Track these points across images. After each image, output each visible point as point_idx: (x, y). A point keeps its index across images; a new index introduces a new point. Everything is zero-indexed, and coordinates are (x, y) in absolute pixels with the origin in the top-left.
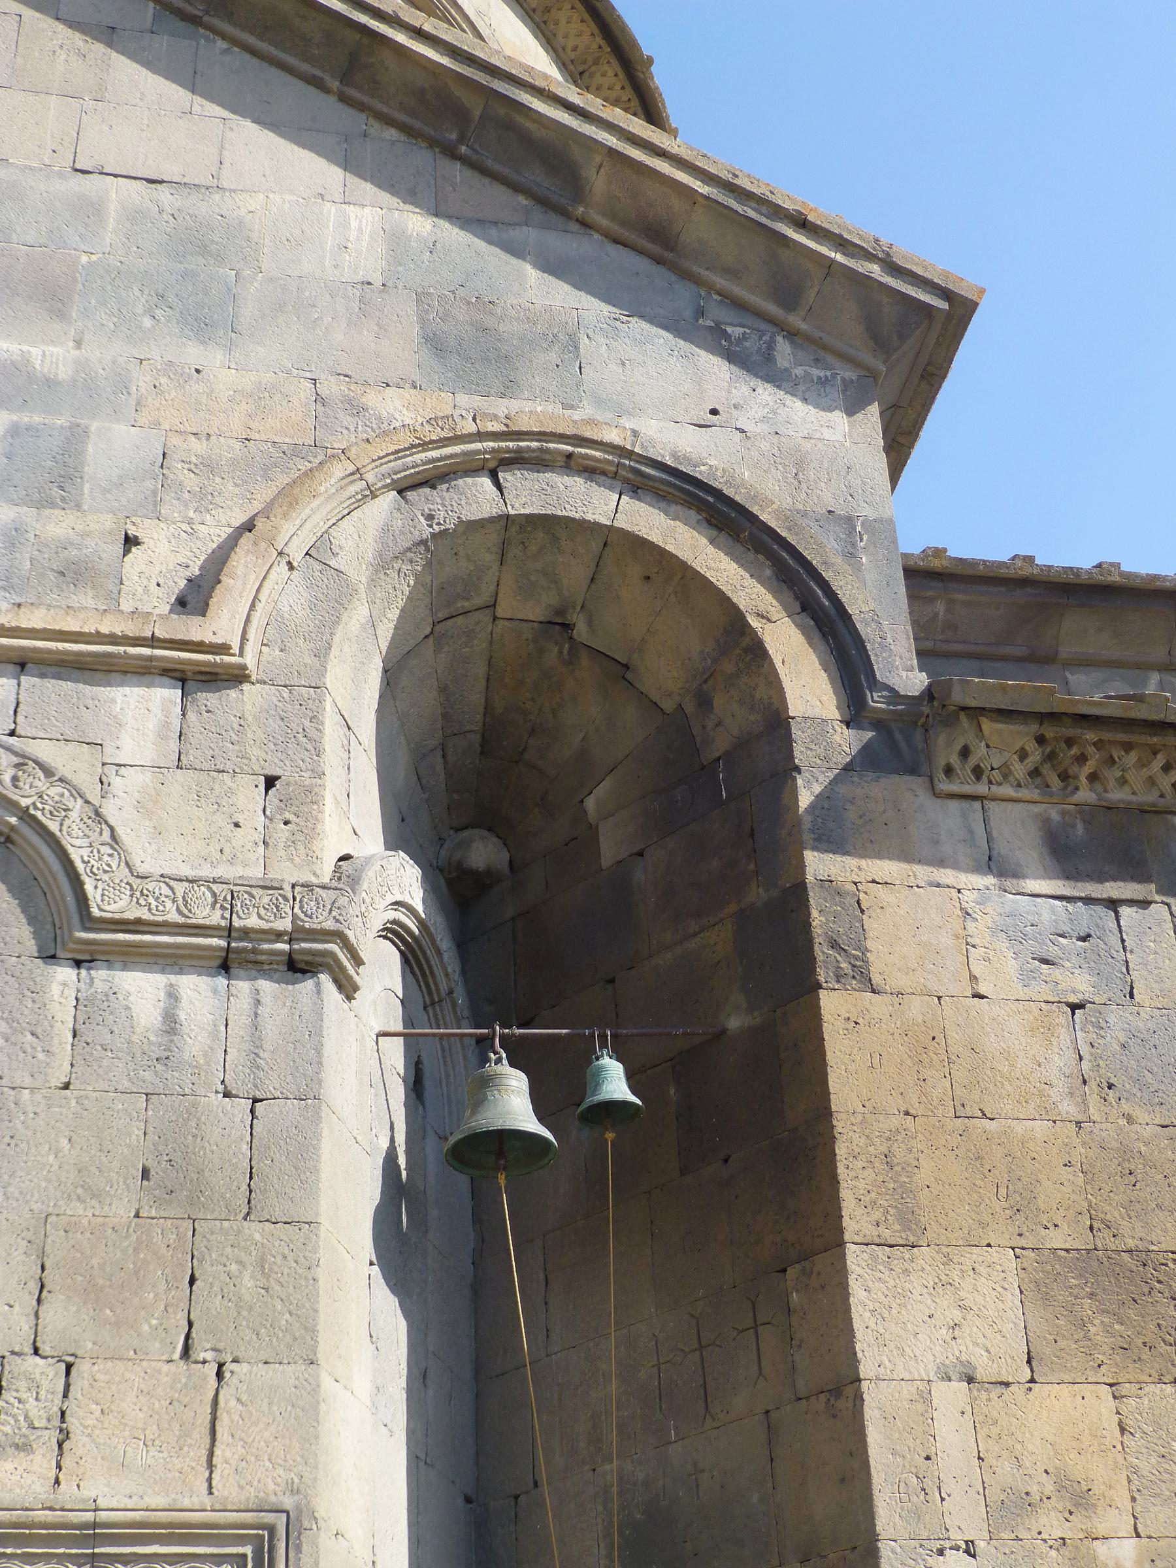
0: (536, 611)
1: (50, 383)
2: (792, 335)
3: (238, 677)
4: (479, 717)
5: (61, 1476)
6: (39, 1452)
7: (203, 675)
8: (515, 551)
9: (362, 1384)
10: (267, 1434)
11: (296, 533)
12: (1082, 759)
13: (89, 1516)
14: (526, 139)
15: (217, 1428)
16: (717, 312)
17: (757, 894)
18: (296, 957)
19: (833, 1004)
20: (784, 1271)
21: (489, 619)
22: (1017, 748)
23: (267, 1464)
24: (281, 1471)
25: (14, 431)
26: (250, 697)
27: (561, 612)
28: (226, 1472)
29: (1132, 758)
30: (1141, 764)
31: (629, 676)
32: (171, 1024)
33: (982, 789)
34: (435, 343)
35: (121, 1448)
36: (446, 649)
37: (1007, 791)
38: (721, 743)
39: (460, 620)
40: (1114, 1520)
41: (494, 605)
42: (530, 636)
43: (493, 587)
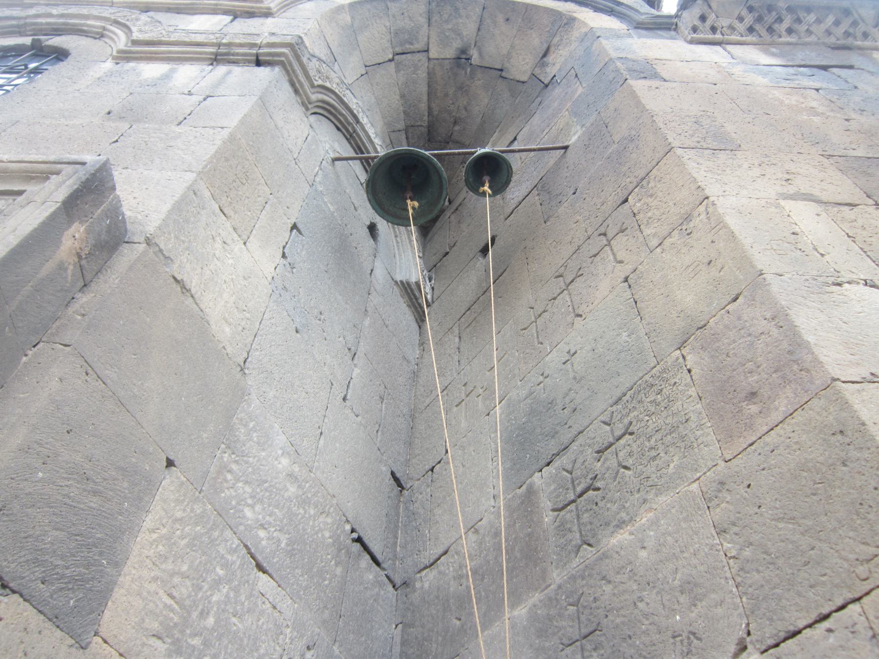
0: (450, 53)
4: (426, 118)
8: (435, 18)
12: (780, 20)
18: (260, 58)
20: (626, 200)
21: (425, 59)
22: (736, 16)
27: (463, 51)
29: (812, 18)
30: (819, 21)
31: (504, 74)
33: (718, 36)
36: (402, 72)
37: (735, 37)
39: (409, 56)
41: (427, 51)
42: (448, 67)
43: (426, 39)
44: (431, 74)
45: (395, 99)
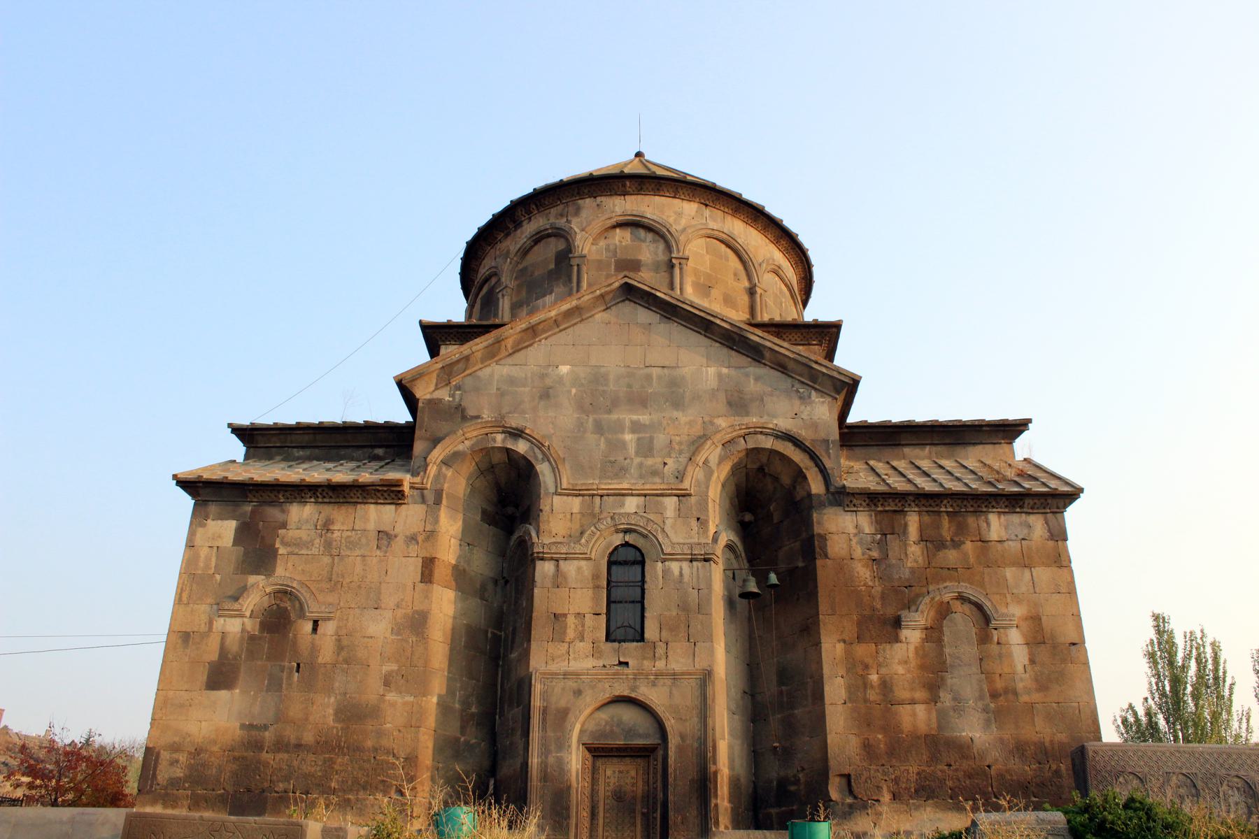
1: (645, 425)
2: (816, 389)
3: (690, 495)
7: (682, 496)
9: (723, 645)
11: (700, 459)
14: (750, 346)
16: (797, 385)
17: (804, 535)
19: (819, 563)
25: (639, 439)
26: (693, 500)
32: (681, 574)
34: (730, 404)
38: (798, 498)
40: (873, 671)
44: (747, 475)
45: (733, 487)
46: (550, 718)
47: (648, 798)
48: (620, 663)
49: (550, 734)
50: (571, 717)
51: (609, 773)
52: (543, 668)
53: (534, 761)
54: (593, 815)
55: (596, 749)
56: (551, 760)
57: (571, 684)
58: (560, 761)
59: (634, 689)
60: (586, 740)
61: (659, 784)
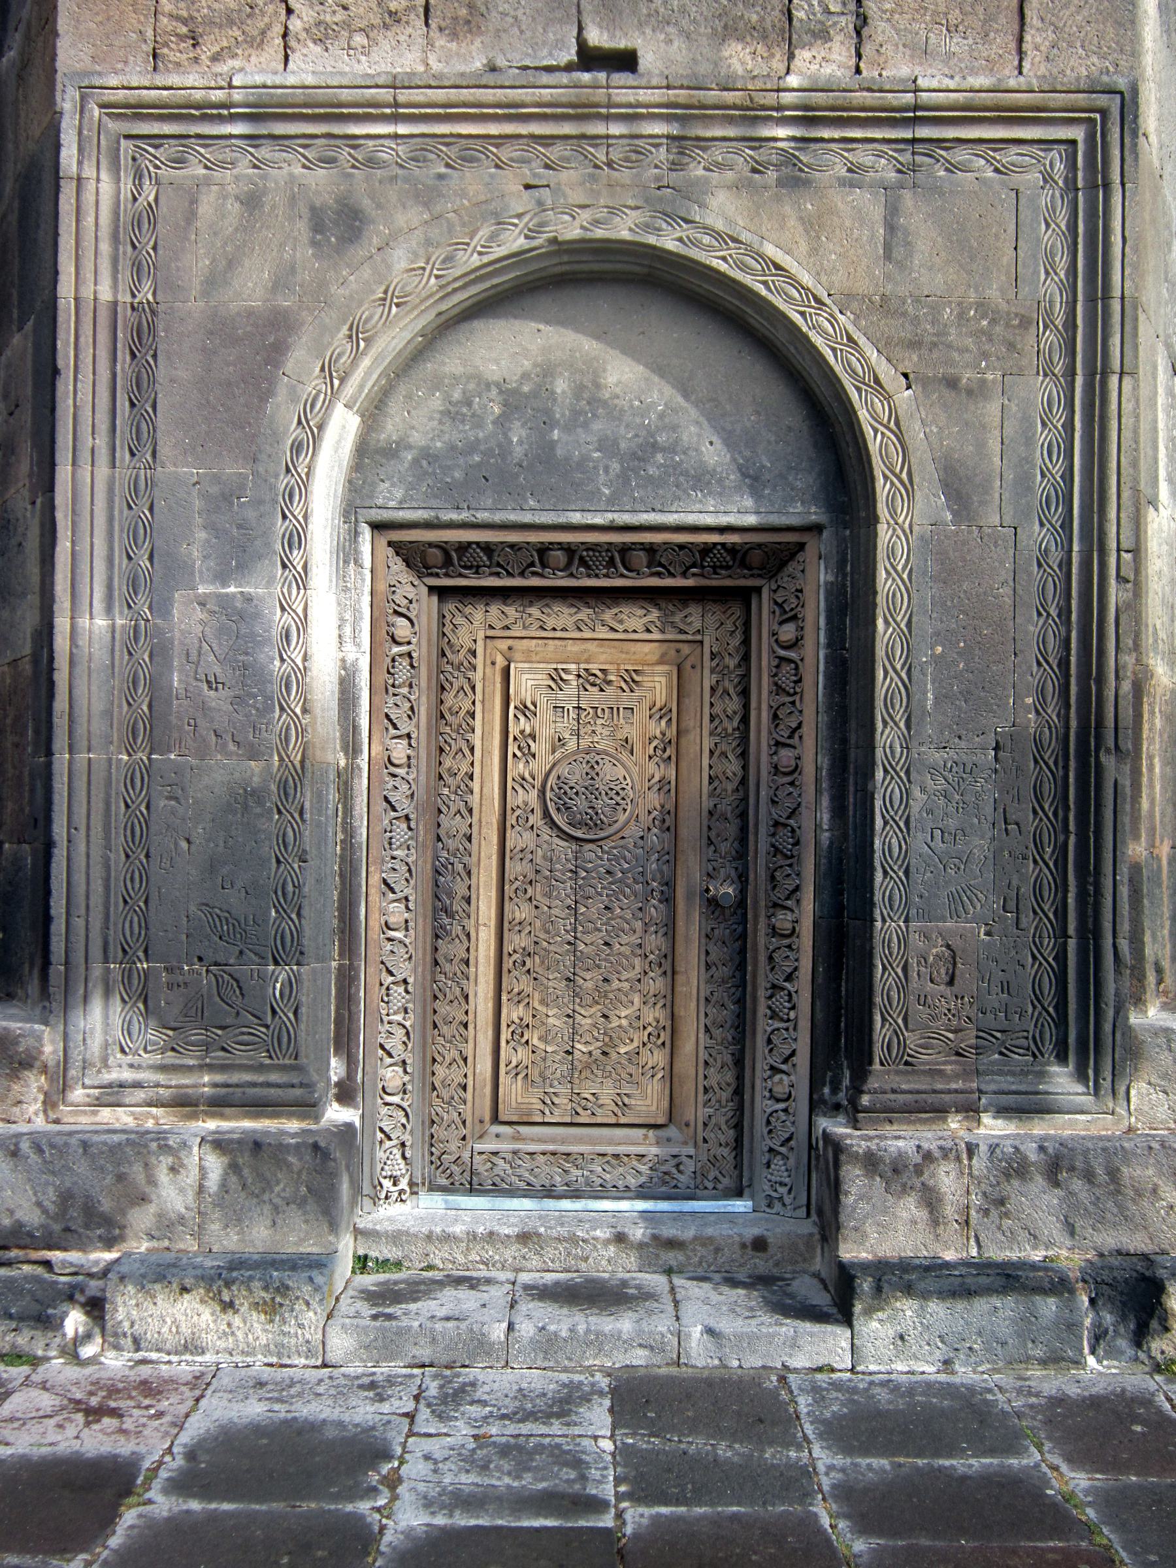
5: (862, 65)
6: (838, 38)
10: (1079, 18)
13: (909, 98)
15: (1026, 11)
23: (1080, 51)
24: (1095, 59)
28: (1037, 59)
35: (923, 33)
46: (176, 375)
47: (739, 824)
48: (589, 58)
49: (179, 468)
50: (301, 364)
51: (527, 683)
52: (130, 77)
53: (88, 626)
54: (443, 910)
55: (454, 556)
56: (187, 619)
57: (292, 171)
58: (238, 620)
59: (673, 201)
60: (392, 498)
61: (811, 755)
